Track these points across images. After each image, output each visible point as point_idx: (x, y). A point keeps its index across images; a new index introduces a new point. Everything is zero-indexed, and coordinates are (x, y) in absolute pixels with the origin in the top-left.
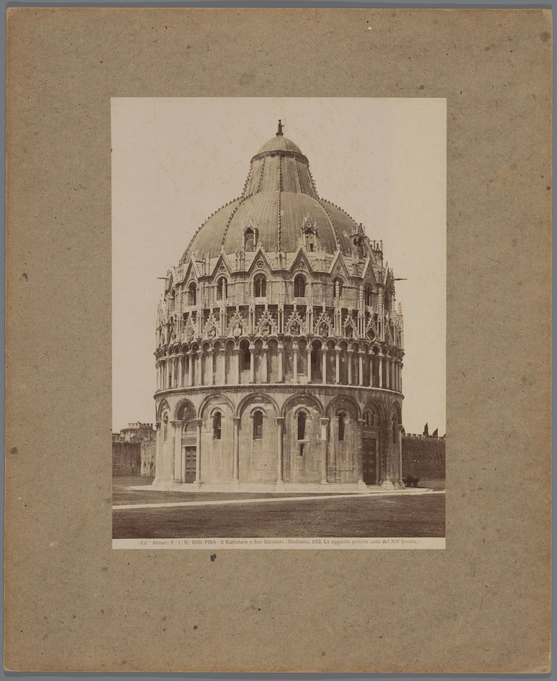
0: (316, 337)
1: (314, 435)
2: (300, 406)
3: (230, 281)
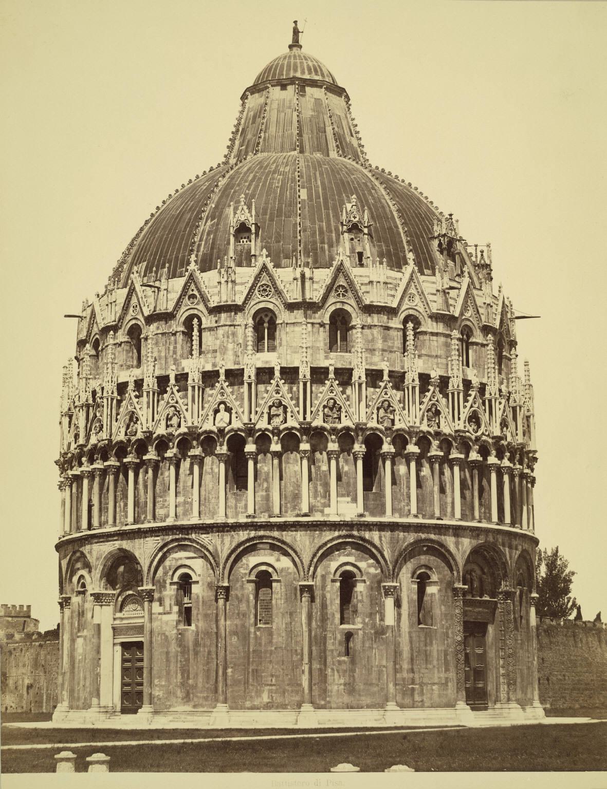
0: (372, 429)
1: (371, 615)
3: (208, 321)
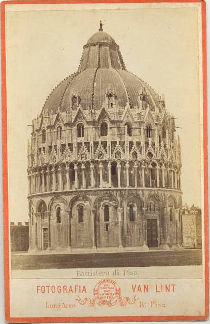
2: (105, 201)
3: (64, 128)
